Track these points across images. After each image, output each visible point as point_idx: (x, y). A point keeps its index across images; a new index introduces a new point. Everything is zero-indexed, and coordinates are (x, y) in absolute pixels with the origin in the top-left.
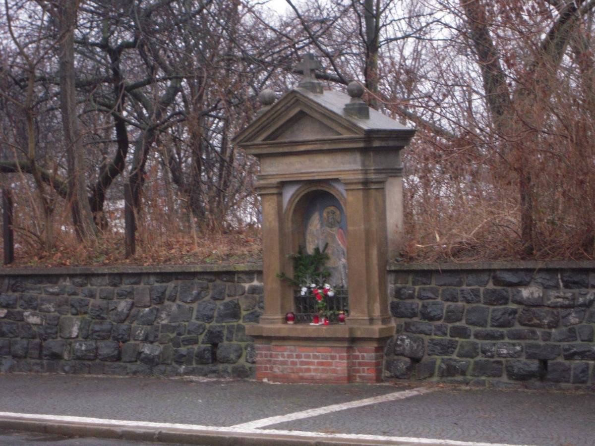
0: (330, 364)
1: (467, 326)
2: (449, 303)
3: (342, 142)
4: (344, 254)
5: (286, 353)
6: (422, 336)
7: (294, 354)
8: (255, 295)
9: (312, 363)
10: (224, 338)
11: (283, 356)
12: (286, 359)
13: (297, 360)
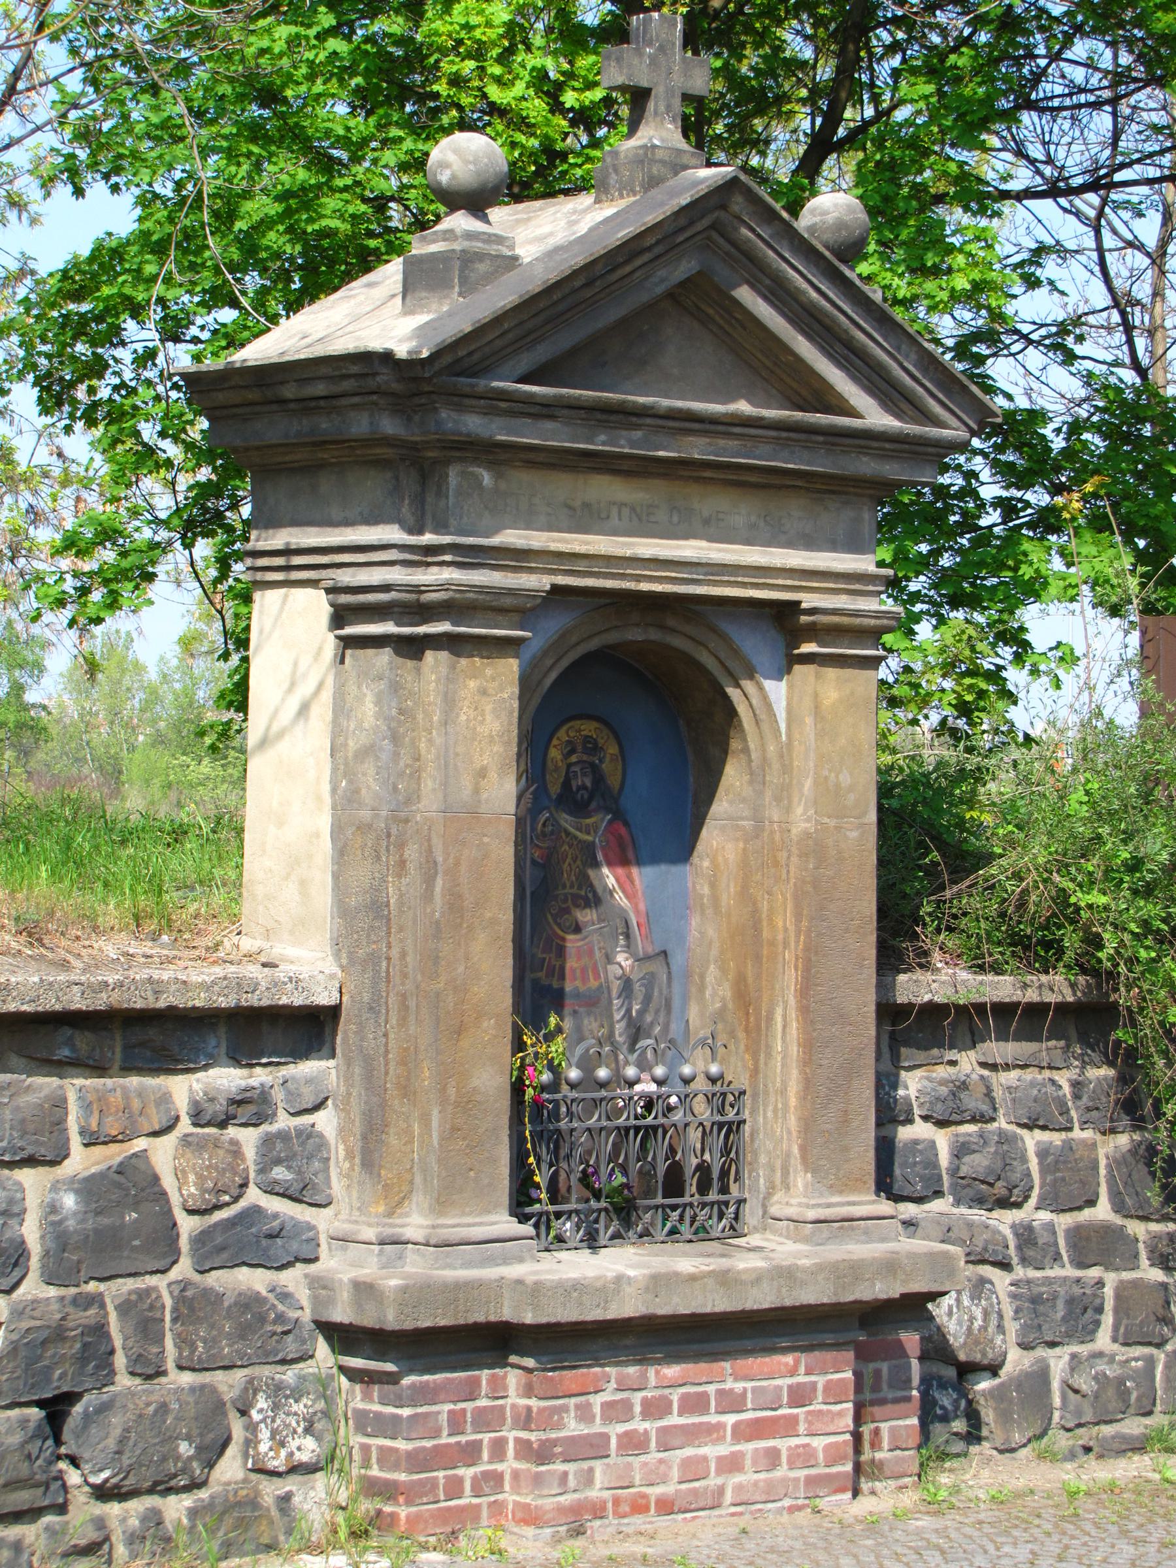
0: (788, 1427)
1: (1118, 1220)
2: (1038, 1134)
3: (863, 450)
4: (627, 936)
5: (597, 1400)
6: (987, 1271)
7: (637, 1398)
8: (232, 1131)
9: (712, 1432)
10: (120, 1360)
11: (585, 1414)
12: (598, 1427)
13: (647, 1425)
